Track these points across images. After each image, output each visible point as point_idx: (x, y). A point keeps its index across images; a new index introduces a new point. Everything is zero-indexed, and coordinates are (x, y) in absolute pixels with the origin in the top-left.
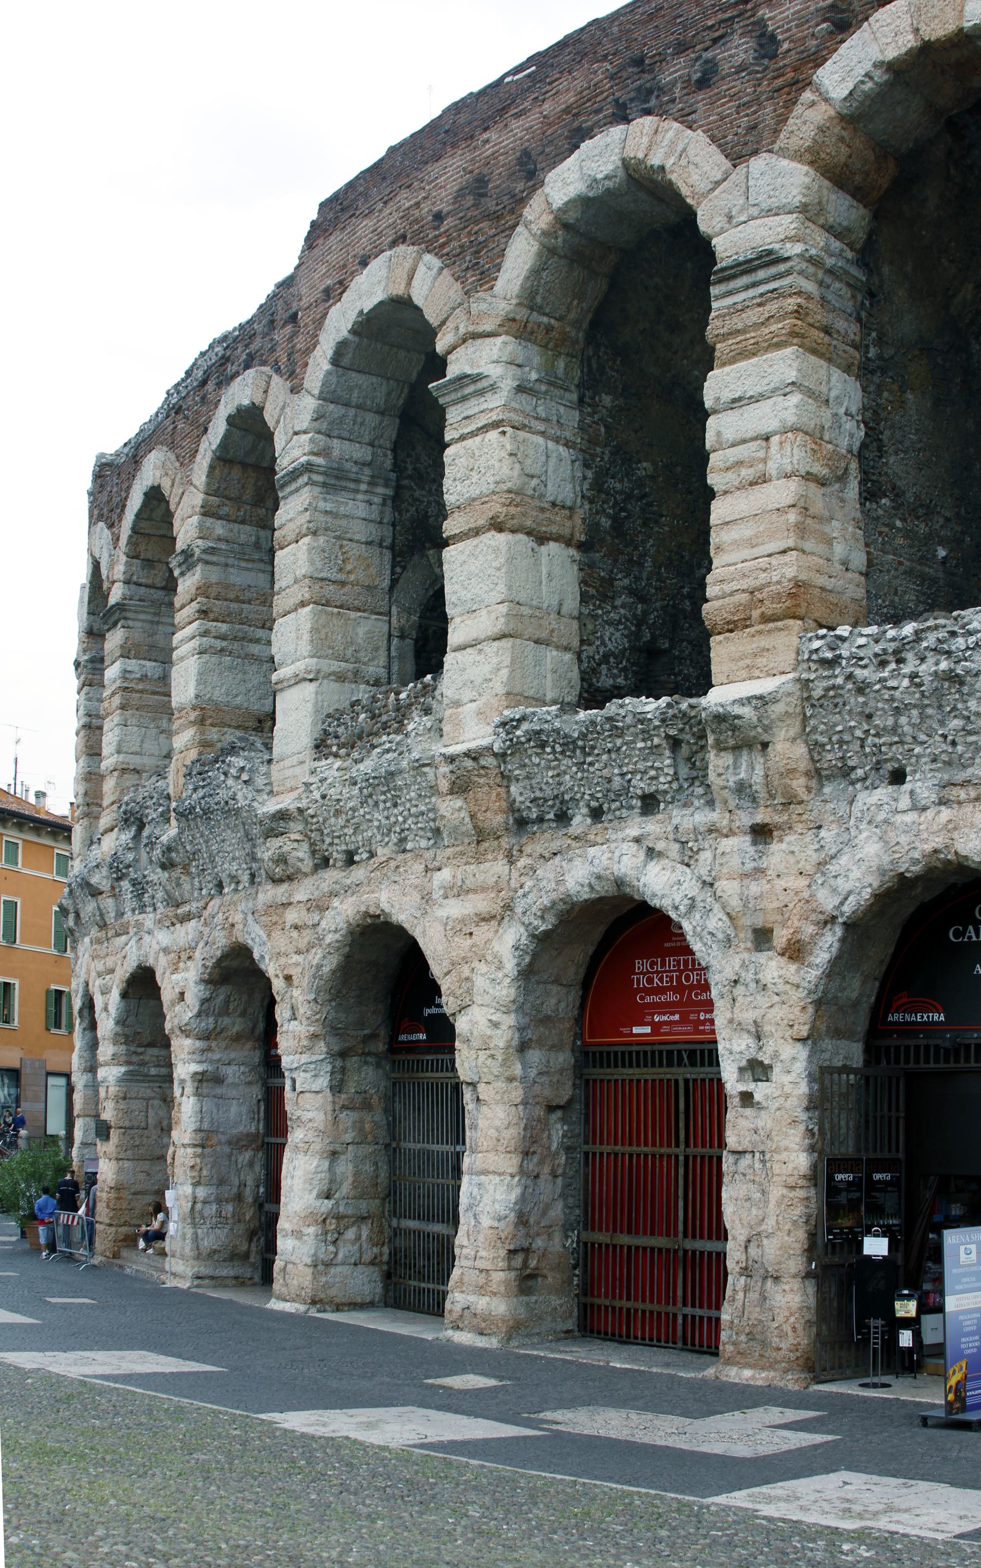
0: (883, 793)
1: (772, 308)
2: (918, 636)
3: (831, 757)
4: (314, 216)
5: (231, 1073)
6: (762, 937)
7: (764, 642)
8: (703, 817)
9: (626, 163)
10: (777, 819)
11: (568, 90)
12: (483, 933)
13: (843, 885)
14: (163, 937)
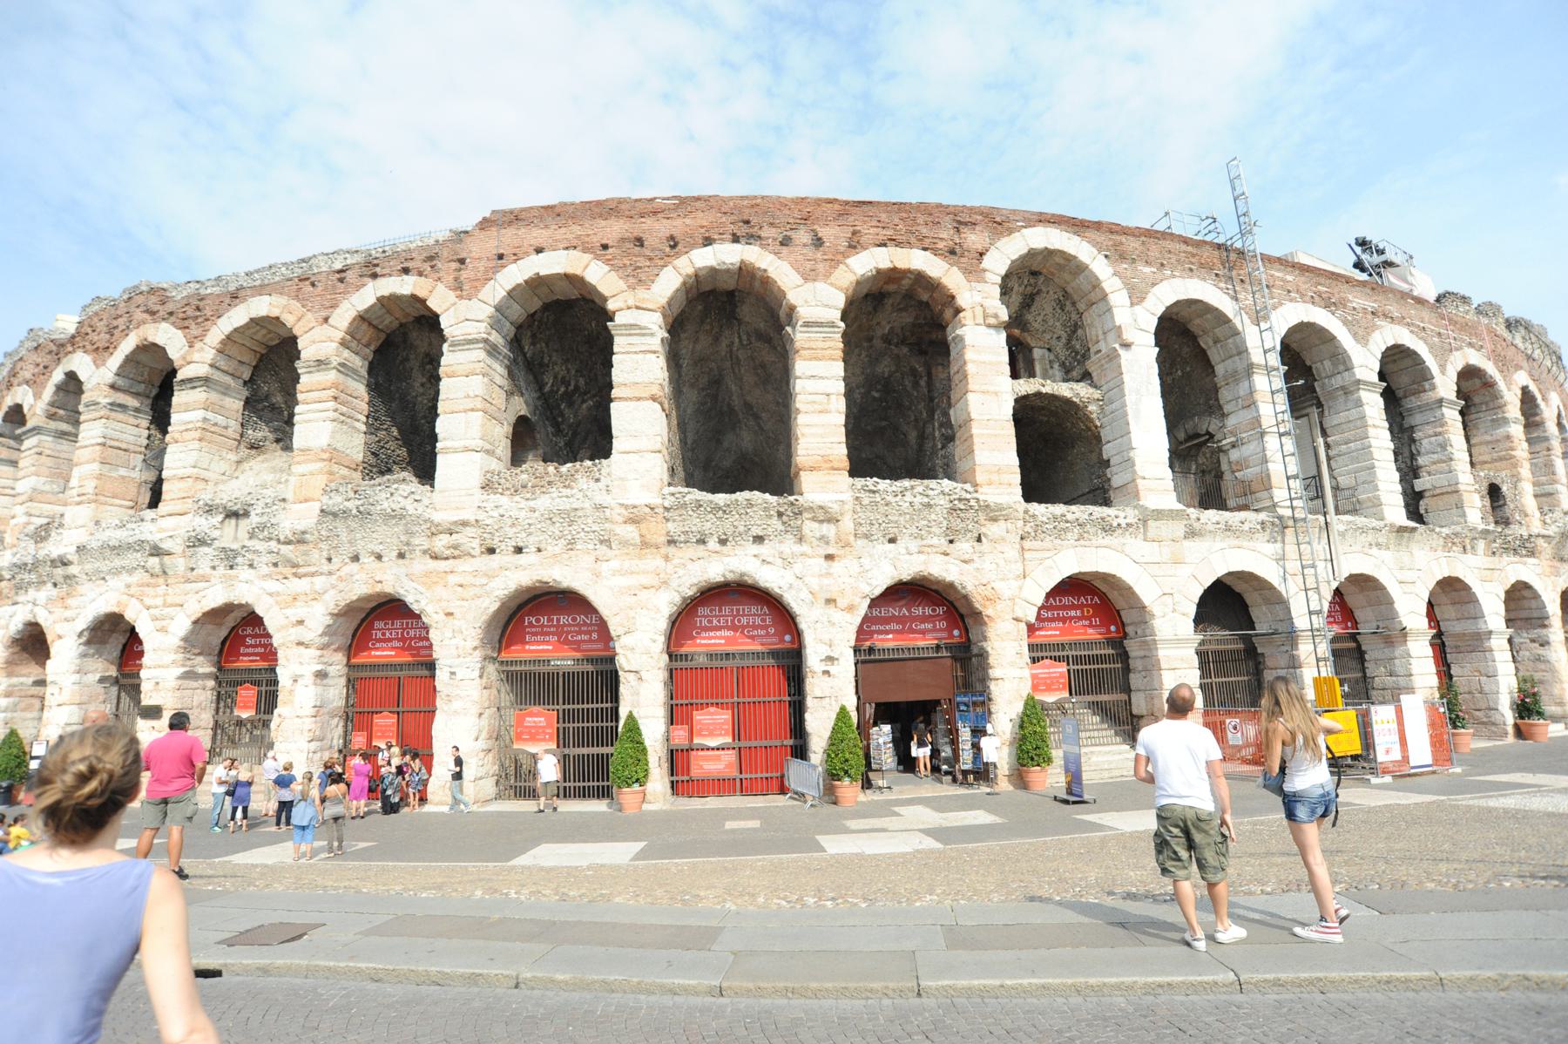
1: (828, 344)
2: (912, 487)
3: (864, 529)
4: (488, 215)
5: (332, 670)
6: (830, 601)
7: (832, 478)
8: (797, 548)
9: (742, 262)
10: (841, 552)
11: (703, 219)
12: (644, 595)
13: (874, 582)
14: (273, 586)
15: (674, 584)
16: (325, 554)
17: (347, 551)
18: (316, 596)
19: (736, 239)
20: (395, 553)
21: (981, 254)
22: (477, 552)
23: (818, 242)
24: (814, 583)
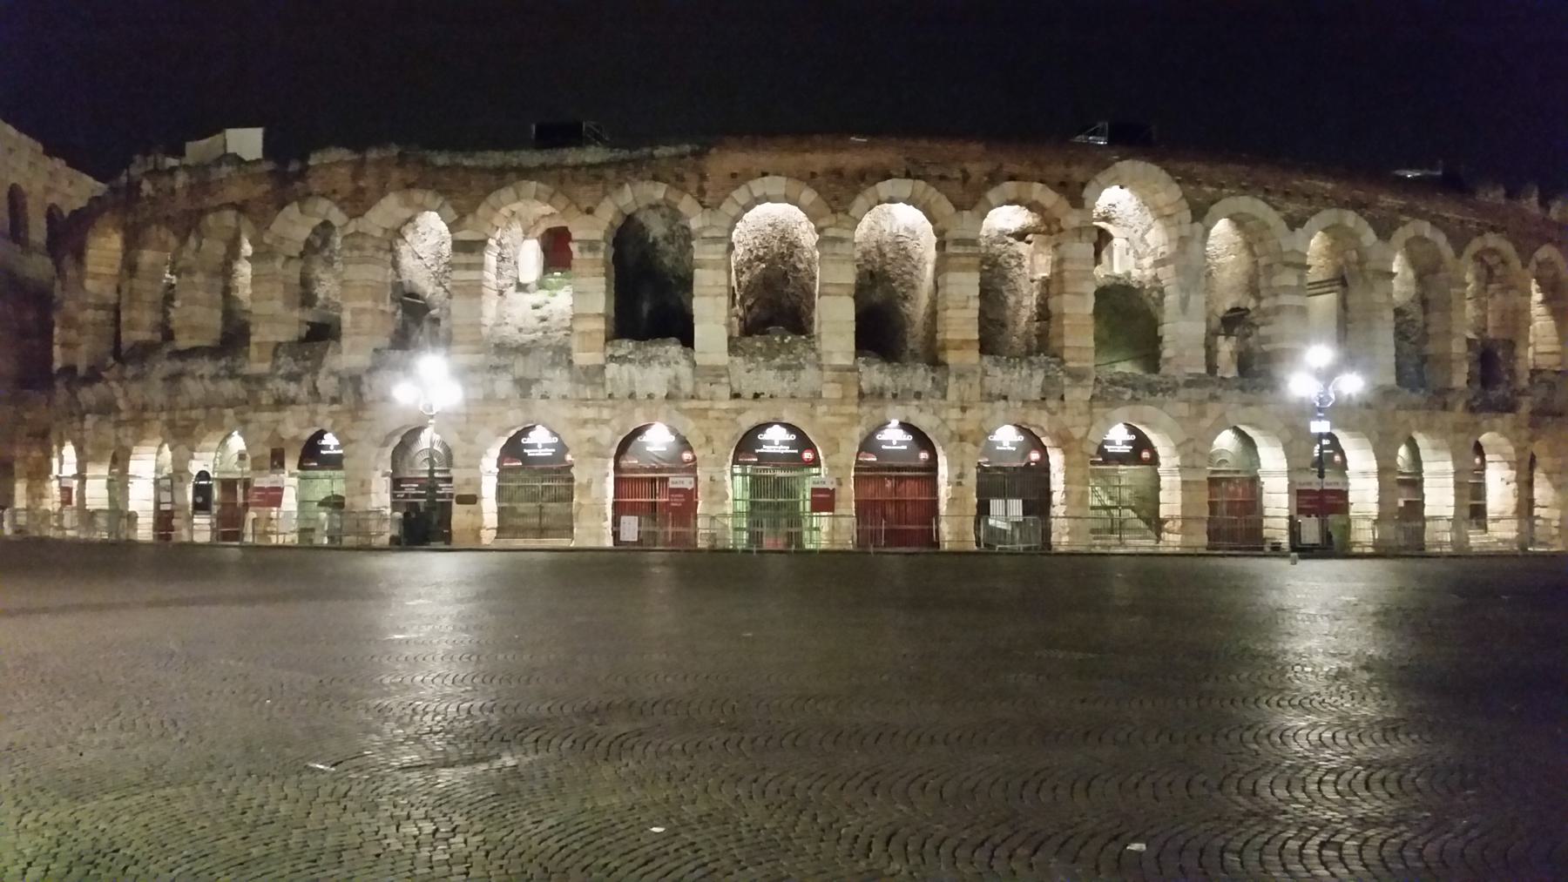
0: (1002, 402)
6: (962, 438)
15: (864, 421)
16: (609, 391)
17: (625, 391)
18: (606, 422)
19: (908, 175)
21: (1083, 185)
23: (966, 177)
24: (953, 426)
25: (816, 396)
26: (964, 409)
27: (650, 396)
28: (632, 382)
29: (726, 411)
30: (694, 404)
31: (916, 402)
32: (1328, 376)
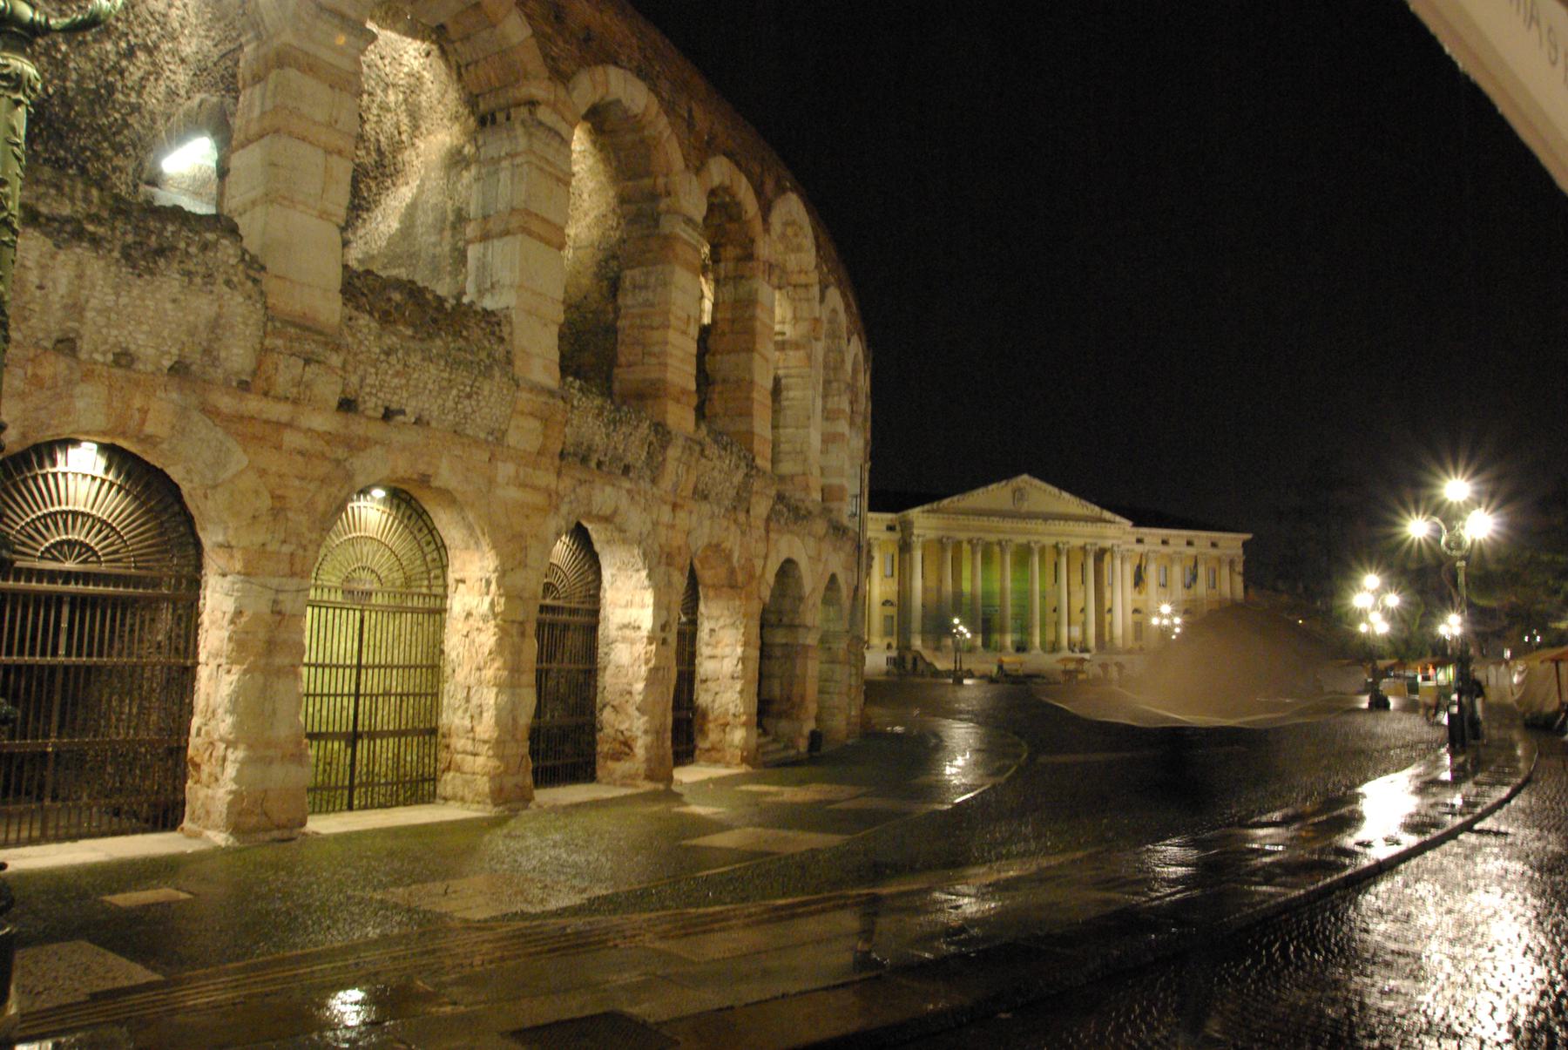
0: (706, 508)
15: (564, 509)
20: (167, 363)
22: (334, 403)
25: (498, 437)
26: (675, 506)
27: (124, 358)
28: (76, 309)
29: (330, 438)
30: (252, 404)
31: (627, 485)
32: (1449, 516)
